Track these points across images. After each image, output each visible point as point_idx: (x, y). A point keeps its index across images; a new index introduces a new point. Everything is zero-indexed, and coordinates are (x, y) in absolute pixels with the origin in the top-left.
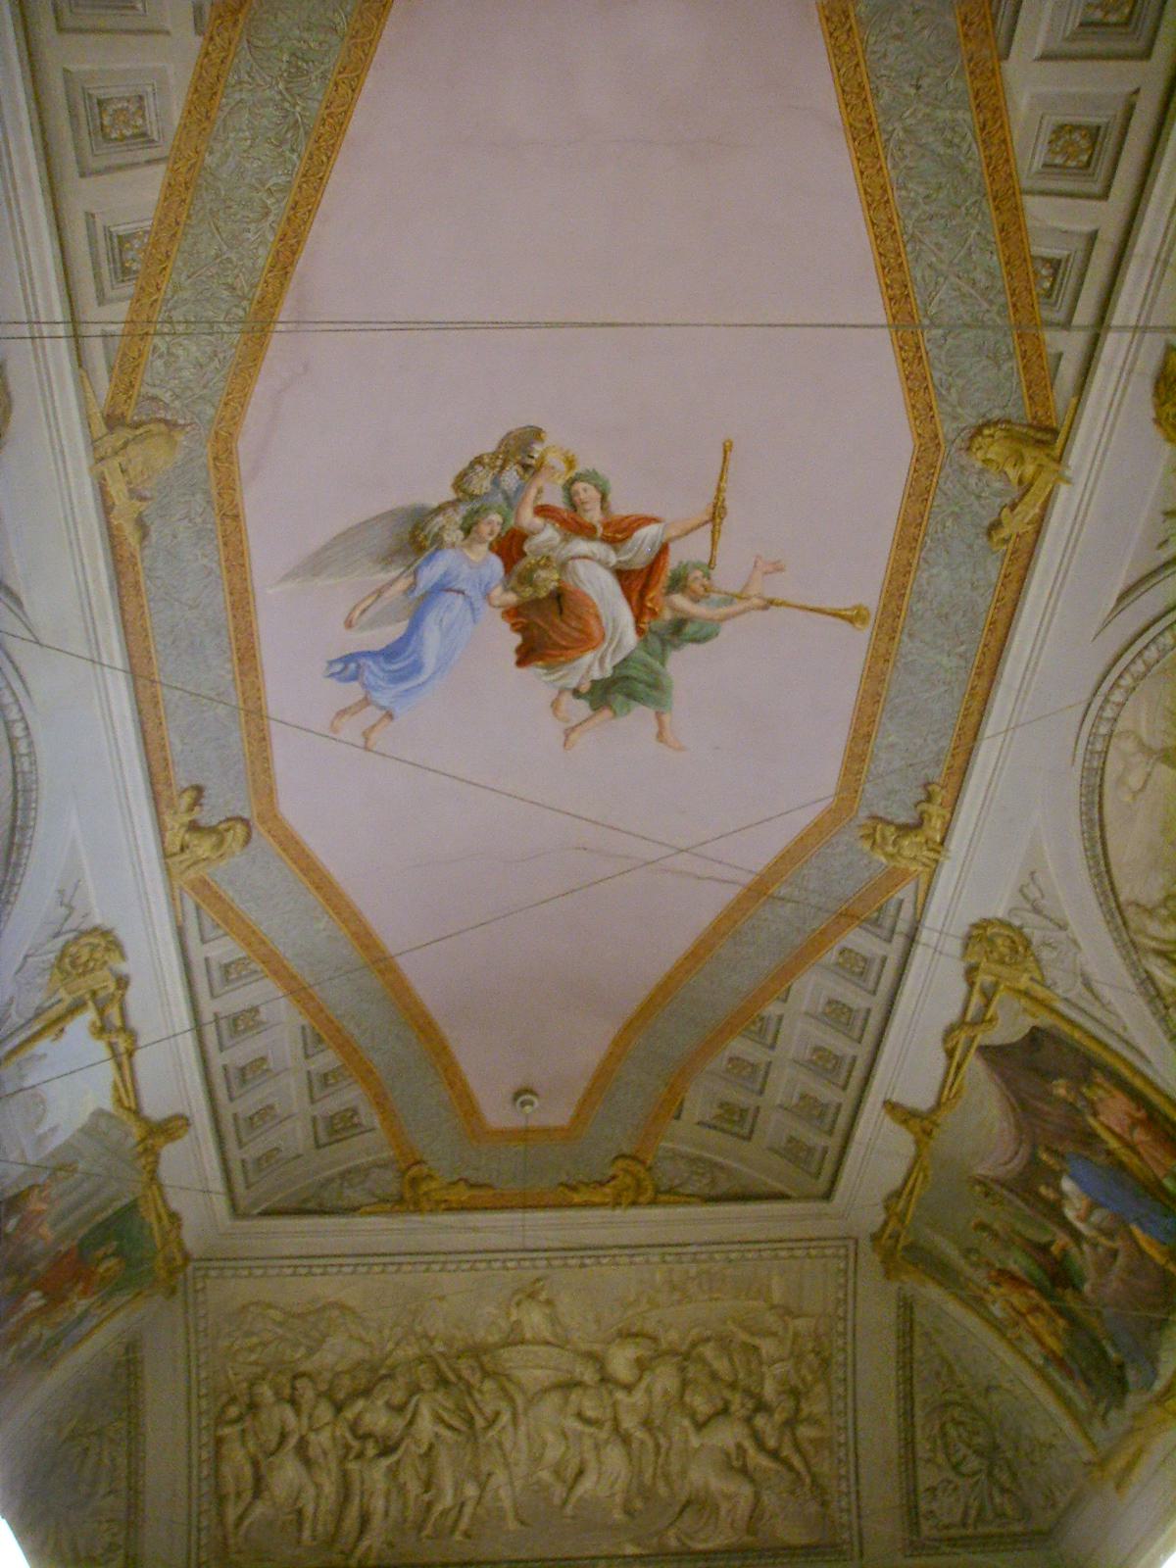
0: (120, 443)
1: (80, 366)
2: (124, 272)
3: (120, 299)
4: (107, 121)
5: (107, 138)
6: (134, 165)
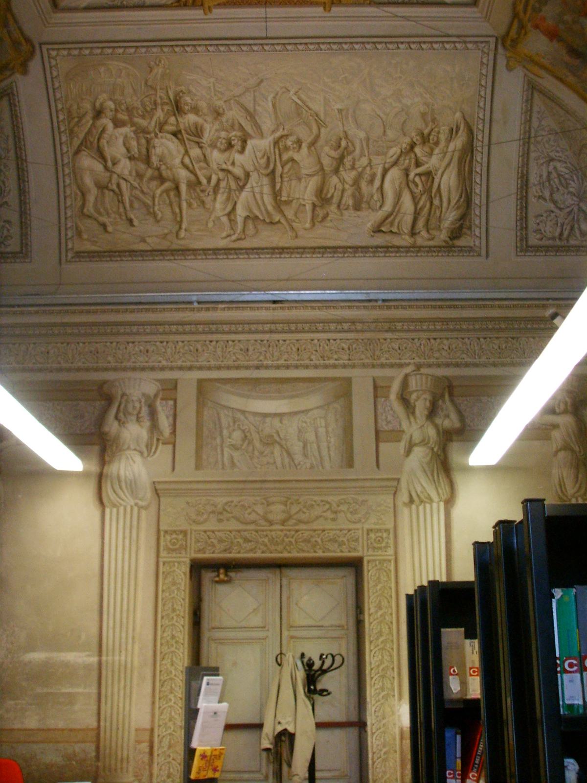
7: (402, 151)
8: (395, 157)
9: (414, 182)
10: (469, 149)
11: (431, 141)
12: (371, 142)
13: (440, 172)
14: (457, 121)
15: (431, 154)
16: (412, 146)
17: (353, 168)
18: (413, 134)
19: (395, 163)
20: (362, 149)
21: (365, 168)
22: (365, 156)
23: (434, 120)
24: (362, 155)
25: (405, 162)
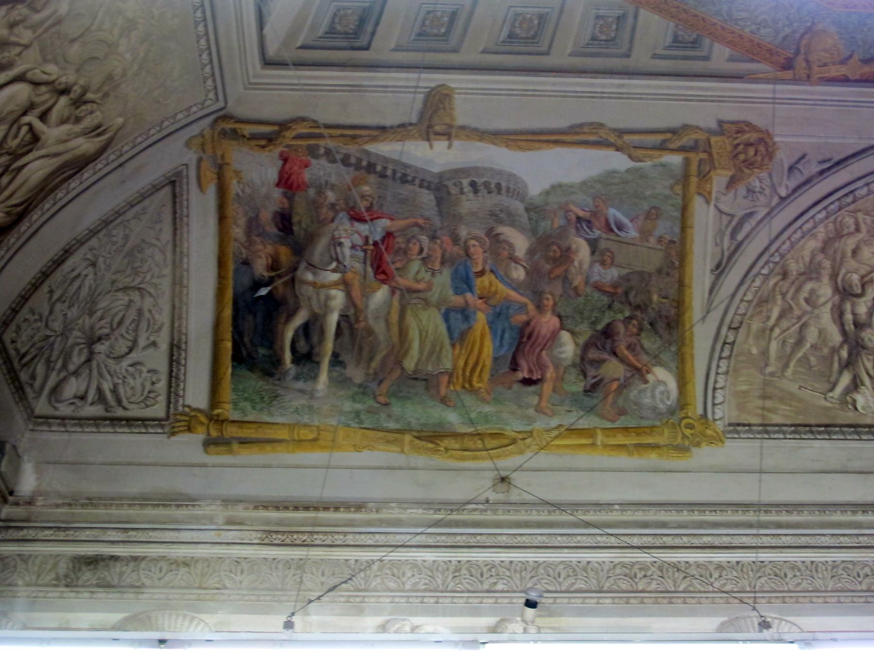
0: (804, 65)
1: (742, 78)
2: (695, 44)
3: (711, 47)
4: (603, 37)
5: (613, 39)
6: (634, 28)
7: (53, 82)
8: (45, 78)
9: (19, 129)
10: (80, 164)
11: (78, 111)
12: (57, 28)
13: (43, 152)
14: (111, 126)
15: (63, 122)
16: (65, 91)
17: (12, 26)
18: (82, 82)
19: (36, 84)
20: (42, 22)
21: (18, 44)
22: (34, 32)
23: (106, 95)
24: (33, 28)
25: (44, 96)
